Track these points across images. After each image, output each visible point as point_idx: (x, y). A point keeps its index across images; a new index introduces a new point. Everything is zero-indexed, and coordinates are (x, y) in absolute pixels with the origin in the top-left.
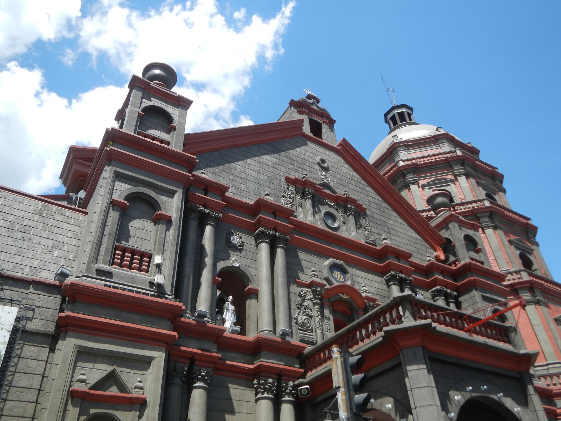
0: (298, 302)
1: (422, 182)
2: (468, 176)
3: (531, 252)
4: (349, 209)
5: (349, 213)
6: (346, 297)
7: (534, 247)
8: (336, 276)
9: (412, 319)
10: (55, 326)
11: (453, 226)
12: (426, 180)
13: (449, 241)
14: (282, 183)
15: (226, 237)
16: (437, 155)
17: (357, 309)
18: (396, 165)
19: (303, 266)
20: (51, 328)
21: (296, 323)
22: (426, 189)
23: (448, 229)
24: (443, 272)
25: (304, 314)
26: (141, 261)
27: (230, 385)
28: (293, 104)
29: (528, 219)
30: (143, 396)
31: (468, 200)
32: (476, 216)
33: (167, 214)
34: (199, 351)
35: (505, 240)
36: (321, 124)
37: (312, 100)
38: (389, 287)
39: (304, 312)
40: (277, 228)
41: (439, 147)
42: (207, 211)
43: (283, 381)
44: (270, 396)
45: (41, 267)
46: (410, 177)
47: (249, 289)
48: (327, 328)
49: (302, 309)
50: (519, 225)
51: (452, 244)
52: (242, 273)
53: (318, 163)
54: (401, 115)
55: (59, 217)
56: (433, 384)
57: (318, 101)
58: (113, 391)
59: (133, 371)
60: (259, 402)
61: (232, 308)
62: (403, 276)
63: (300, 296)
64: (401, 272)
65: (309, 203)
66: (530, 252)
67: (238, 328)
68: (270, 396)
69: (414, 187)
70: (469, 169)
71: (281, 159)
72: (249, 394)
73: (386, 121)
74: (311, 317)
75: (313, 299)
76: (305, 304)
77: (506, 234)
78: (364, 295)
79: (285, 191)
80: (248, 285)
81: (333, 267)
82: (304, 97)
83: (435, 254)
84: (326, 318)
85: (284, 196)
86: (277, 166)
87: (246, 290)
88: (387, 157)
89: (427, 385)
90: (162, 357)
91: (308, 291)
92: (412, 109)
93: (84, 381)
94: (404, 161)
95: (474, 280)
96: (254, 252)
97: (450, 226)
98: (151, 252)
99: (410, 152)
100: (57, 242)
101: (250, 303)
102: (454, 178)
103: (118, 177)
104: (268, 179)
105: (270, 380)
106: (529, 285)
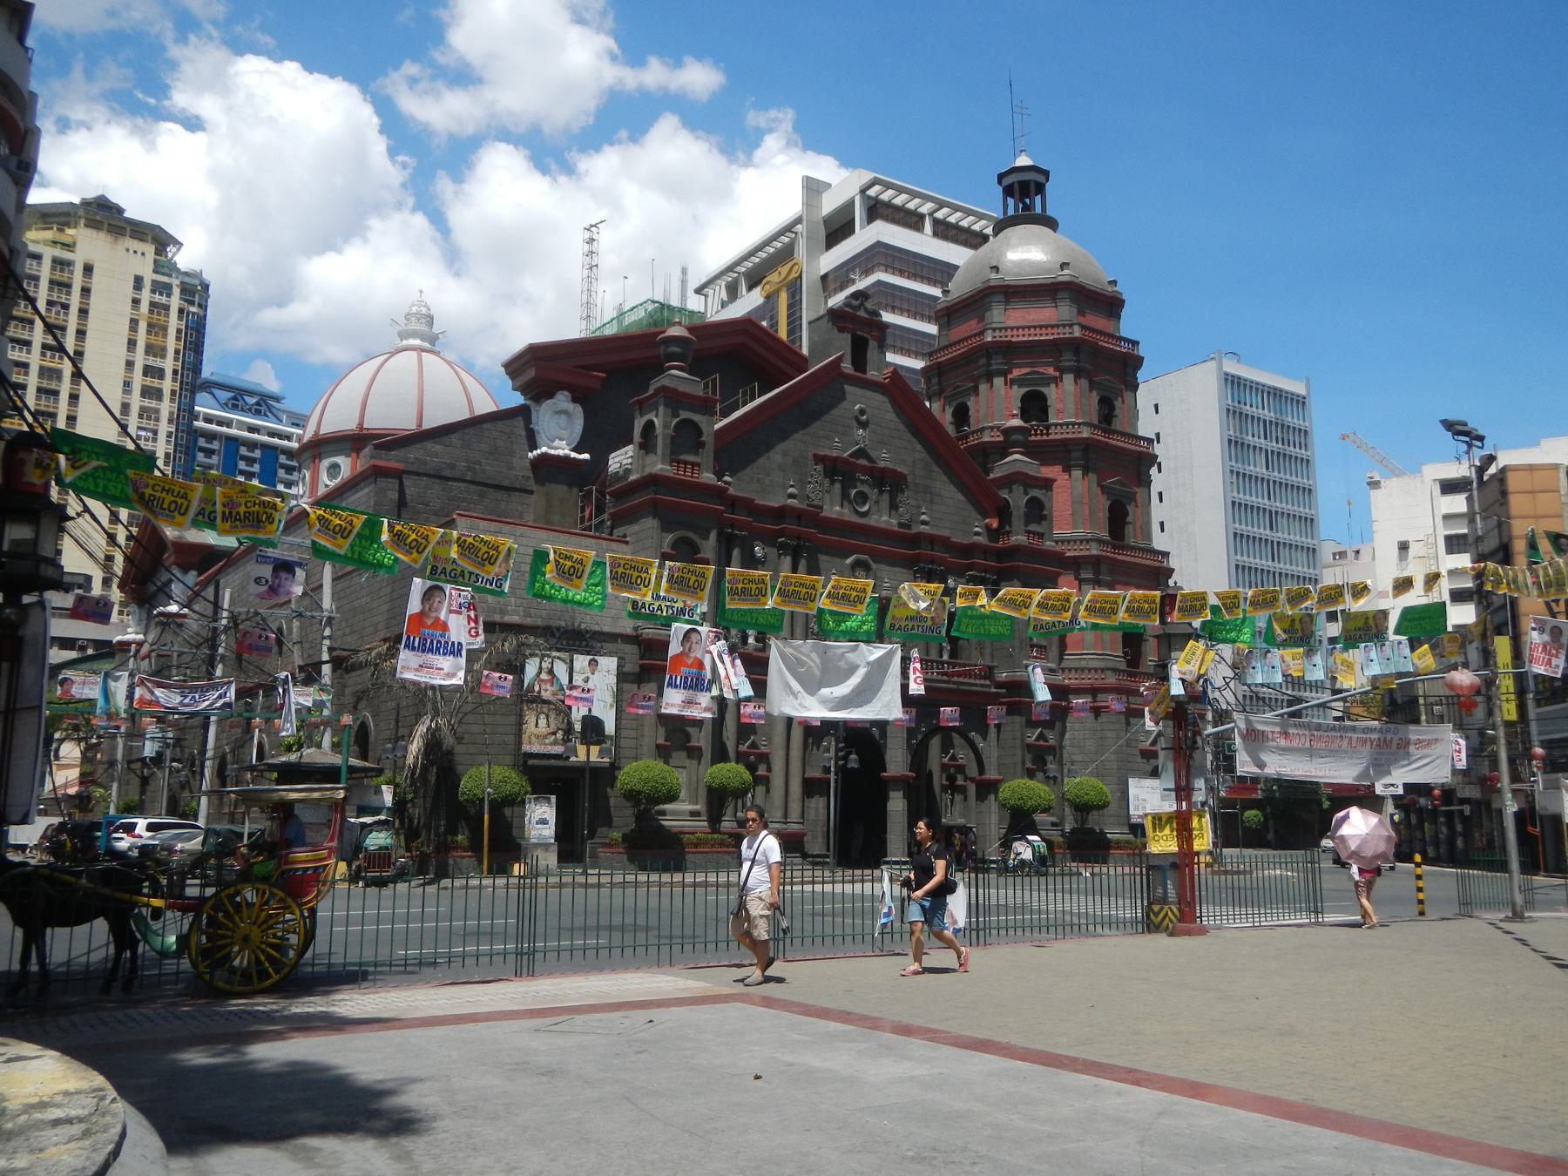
2: (1078, 373)
3: (1132, 498)
11: (1018, 489)
18: (982, 333)
20: (637, 669)
23: (1011, 491)
24: (985, 551)
36: (867, 340)
46: (997, 363)
64: (932, 562)
69: (999, 382)
92: (1046, 174)
94: (994, 330)
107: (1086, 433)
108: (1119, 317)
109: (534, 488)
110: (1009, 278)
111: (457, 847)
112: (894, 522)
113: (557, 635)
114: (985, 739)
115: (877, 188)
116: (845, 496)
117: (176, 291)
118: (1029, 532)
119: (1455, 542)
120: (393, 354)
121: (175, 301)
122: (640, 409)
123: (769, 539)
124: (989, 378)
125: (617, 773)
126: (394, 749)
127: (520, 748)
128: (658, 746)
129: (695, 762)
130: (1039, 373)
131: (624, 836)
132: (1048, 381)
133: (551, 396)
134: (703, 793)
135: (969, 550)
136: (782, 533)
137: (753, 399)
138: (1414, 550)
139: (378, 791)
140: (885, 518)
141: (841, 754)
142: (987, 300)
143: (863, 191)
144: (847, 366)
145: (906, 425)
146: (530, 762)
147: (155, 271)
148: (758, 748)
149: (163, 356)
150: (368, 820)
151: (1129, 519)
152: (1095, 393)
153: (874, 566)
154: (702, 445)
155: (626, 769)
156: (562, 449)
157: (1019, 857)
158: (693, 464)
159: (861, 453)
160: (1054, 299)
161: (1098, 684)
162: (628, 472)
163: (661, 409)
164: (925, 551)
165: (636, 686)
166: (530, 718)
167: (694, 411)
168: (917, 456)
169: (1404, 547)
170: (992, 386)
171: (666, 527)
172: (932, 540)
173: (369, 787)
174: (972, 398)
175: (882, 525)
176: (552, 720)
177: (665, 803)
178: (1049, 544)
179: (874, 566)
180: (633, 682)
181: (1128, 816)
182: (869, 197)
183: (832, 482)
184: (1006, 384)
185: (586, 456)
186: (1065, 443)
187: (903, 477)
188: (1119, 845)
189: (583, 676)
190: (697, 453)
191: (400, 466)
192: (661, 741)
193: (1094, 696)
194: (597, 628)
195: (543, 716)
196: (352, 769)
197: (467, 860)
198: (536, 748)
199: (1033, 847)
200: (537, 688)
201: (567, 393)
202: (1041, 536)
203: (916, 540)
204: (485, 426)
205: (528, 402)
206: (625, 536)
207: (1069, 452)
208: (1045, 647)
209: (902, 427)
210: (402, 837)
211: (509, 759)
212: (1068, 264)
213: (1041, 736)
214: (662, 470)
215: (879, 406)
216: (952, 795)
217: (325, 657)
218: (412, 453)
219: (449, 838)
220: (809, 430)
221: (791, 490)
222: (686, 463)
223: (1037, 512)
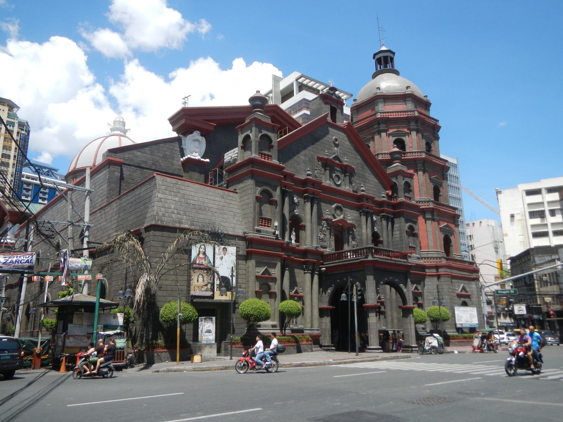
2: (418, 131)
3: (441, 185)
11: (400, 178)
13: (395, 183)
18: (375, 114)
20: (245, 254)
21: (319, 239)
23: (397, 178)
24: (389, 205)
26: (268, 222)
30: (276, 276)
33: (275, 199)
34: (286, 256)
36: (336, 109)
38: (361, 215)
46: (382, 127)
54: (386, 58)
55: (230, 198)
58: (267, 276)
60: (306, 274)
61: (294, 234)
64: (368, 208)
67: (298, 244)
69: (384, 135)
73: (374, 58)
74: (325, 235)
81: (337, 208)
85: (316, 170)
88: (370, 102)
92: (394, 53)
93: (258, 272)
94: (381, 113)
95: (403, 211)
97: (399, 177)
98: (271, 218)
107: (424, 156)
108: (429, 110)
109: (183, 174)
110: (385, 93)
111: (157, 346)
112: (351, 190)
114: (406, 287)
115: (303, 79)
116: (331, 176)
117: (16, 125)
118: (405, 197)
119: (532, 214)
120: (107, 137)
121: (16, 129)
122: (241, 131)
123: (301, 194)
124: (379, 133)
125: (237, 306)
126: (124, 294)
127: (189, 293)
128: (256, 292)
129: (273, 300)
130: (402, 131)
131: (241, 338)
133: (192, 133)
134: (277, 315)
135: (381, 204)
136: (306, 191)
137: (285, 134)
138: (517, 217)
139: (115, 317)
140: (347, 188)
141: (359, 293)
142: (376, 101)
143: (297, 80)
144: (329, 119)
145: (354, 148)
146: (195, 300)
147: (7, 117)
148: (299, 294)
149: (10, 150)
150: (111, 332)
151: (441, 194)
152: (424, 140)
153: (344, 209)
154: (272, 147)
155: (243, 303)
156: (197, 156)
157: (431, 345)
158: (268, 156)
159: (336, 158)
160: (405, 101)
161: (439, 264)
162: (235, 160)
163: (254, 129)
164: (365, 203)
165: (244, 262)
166: (194, 277)
167: (268, 131)
168: (359, 161)
169: (512, 216)
170: (381, 136)
171: (258, 184)
172: (368, 198)
173: (109, 314)
174: (371, 142)
175: (347, 191)
176: (205, 278)
177: (261, 321)
178: (413, 202)
179: (344, 209)
180: (243, 260)
181: (456, 324)
182: (299, 83)
183: (325, 170)
184: (387, 136)
185: (208, 160)
186: (415, 160)
187: (353, 169)
188: (454, 338)
190: (270, 151)
191: (121, 160)
192: (257, 289)
193: (437, 270)
194: (226, 232)
195: (200, 276)
196: (102, 305)
197: (165, 354)
198: (197, 293)
199: (438, 340)
200: (198, 262)
201: (198, 132)
202: (410, 198)
203: (360, 198)
204: (161, 145)
205: (181, 136)
206: (235, 190)
207: (416, 164)
208: (414, 248)
209: (352, 148)
210: (130, 342)
211: (184, 298)
212: (409, 87)
213: (416, 288)
214: (255, 156)
215: (342, 137)
216: (379, 316)
217: (85, 246)
218: (127, 155)
219: (154, 342)
220: (314, 146)
221: (308, 172)
222: (265, 155)
223: (408, 188)
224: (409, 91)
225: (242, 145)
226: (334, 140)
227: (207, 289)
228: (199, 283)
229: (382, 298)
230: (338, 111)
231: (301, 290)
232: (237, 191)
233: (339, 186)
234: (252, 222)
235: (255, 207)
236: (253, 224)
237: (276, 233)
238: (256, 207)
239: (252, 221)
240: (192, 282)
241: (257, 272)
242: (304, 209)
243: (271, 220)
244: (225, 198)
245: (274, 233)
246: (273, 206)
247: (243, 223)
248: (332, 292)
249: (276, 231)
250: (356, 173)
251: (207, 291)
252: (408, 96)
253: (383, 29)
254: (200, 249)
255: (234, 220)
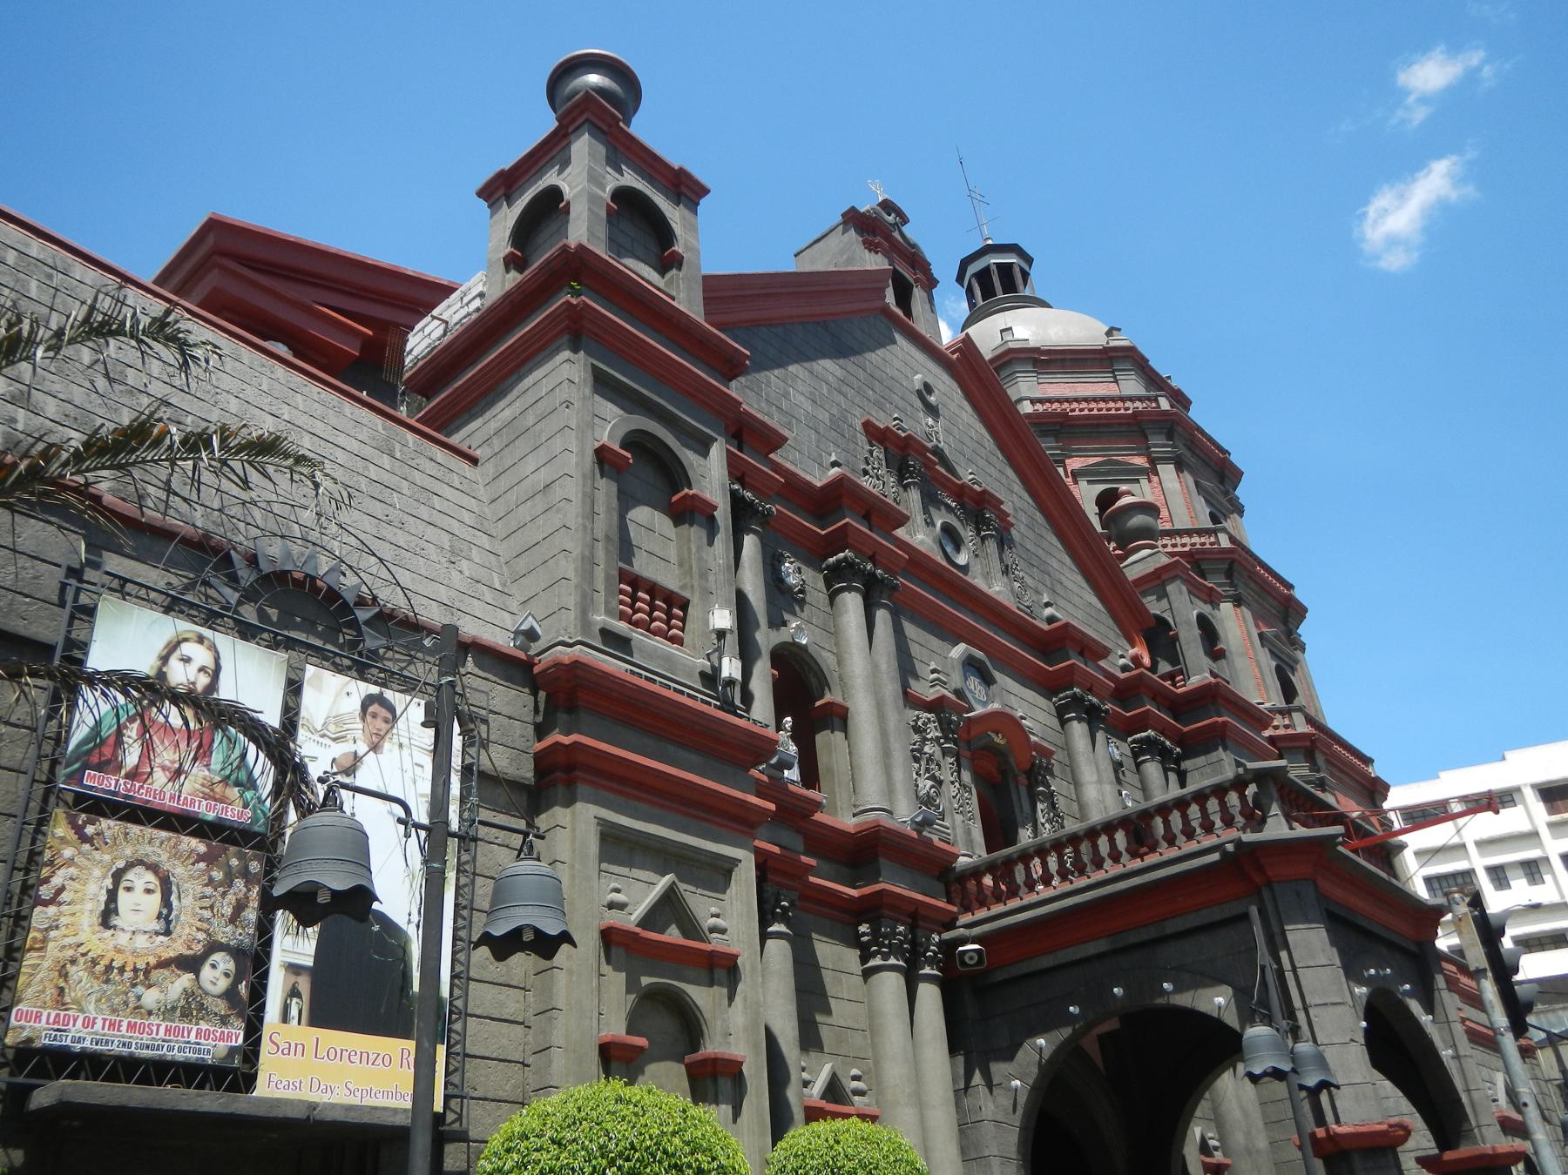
0: (914, 744)
1: (1075, 463)
2: (1180, 466)
4: (987, 523)
5: (984, 531)
6: (1002, 742)
7: (1298, 653)
8: (972, 687)
9: (1283, 820)
10: (533, 766)
12: (1082, 459)
13: (1161, 622)
14: (859, 435)
15: (773, 565)
16: (1104, 399)
17: (1017, 771)
19: (913, 655)
20: (527, 773)
22: (1083, 484)
23: (1163, 595)
25: (927, 775)
26: (670, 616)
27: (814, 936)
28: (855, 220)
29: (1290, 587)
30: (733, 950)
31: (1178, 526)
32: (1199, 567)
34: (776, 850)
35: (1255, 633)
37: (893, 215)
38: (1063, 722)
39: (927, 770)
40: (877, 557)
41: (1112, 380)
42: (748, 495)
43: (920, 932)
44: (901, 963)
45: (457, 605)
47: (830, 704)
48: (969, 812)
49: (923, 763)
50: (1274, 597)
51: (1171, 633)
52: (813, 664)
53: (919, 392)
54: (1005, 270)
55: (429, 467)
56: (1338, 963)
57: (905, 220)
58: (673, 935)
59: (699, 891)
60: (875, 978)
62: (1095, 700)
63: (917, 729)
65: (914, 496)
66: (1291, 663)
68: (901, 963)
70: (1182, 450)
71: (850, 369)
72: (851, 956)
74: (940, 783)
75: (942, 741)
76: (926, 749)
77: (1257, 617)
78: (1033, 738)
79: (866, 458)
80: (822, 697)
81: (970, 664)
82: (874, 205)
83: (1132, 651)
84: (965, 787)
85: (866, 473)
86: (845, 389)
87: (818, 704)
89: (1330, 963)
90: (751, 860)
91: (929, 719)
92: (1029, 261)
93: (621, 906)
94: (1033, 401)
95: (1225, 723)
96: (826, 609)
97: (1170, 588)
98: (686, 594)
99: (1044, 378)
100: (455, 538)
101: (828, 742)
102: (1147, 465)
103: (603, 384)
104: (831, 420)
105: (901, 928)
106: (1308, 744)
113: (246, 576)
119: (1436, 885)
123: (814, 553)
132: (1134, 474)
153: (997, 675)
179: (997, 675)
189: (340, 750)
192: (616, 1028)
194: (391, 598)
195: (141, 878)
212: (1119, 330)
224: (1119, 341)
225: (509, 249)
226: (918, 385)
227: (188, 994)
228: (123, 939)
229: (1216, 1148)
230: (918, 294)
231: (856, 1078)
232: (478, 453)
233: (965, 569)
234: (574, 581)
235: (590, 501)
236: (584, 596)
237: (725, 673)
238: (600, 508)
239: (571, 574)
240: (40, 916)
241: (612, 906)
242: (834, 632)
243: (685, 605)
244: (398, 455)
245: (710, 678)
246: (695, 529)
247: (514, 605)
248: (1034, 1089)
249: (725, 661)
250: (1017, 545)
251: (186, 1014)
252: (1120, 354)
253: (981, 199)
254: (165, 659)
255: (455, 574)
